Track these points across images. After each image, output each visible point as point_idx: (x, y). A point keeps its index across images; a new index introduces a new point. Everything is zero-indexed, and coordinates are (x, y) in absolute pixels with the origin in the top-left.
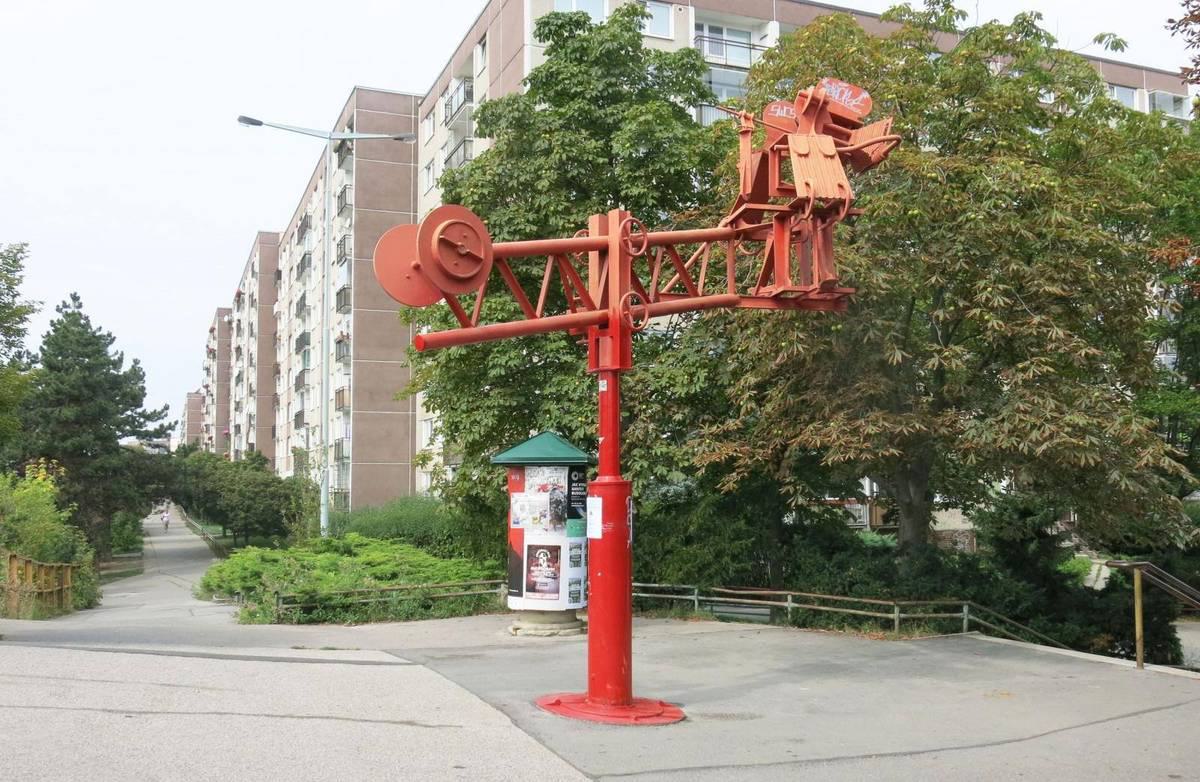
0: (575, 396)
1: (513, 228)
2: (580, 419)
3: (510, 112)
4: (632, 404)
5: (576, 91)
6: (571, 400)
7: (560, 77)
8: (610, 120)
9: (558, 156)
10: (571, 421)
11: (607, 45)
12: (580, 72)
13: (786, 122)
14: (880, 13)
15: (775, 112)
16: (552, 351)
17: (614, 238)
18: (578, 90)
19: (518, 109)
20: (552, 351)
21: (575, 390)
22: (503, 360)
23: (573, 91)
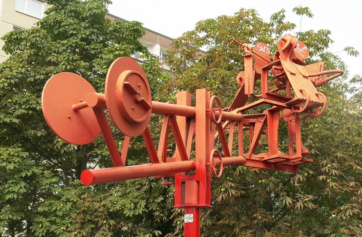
0: (60, 213)
1: (28, 106)
2: (62, 228)
3: (33, 37)
4: (96, 219)
5: (72, 33)
6: (57, 216)
7: (63, 24)
8: (93, 52)
9: (64, 66)
10: (56, 229)
11: (94, 11)
12: (75, 23)
13: (265, 55)
14: (173, 38)
15: (259, 49)
16: (47, 184)
17: (200, 110)
18: (74, 33)
19: (39, 36)
20: (47, 184)
21: (60, 210)
22: (16, 189)
23: (70, 32)
